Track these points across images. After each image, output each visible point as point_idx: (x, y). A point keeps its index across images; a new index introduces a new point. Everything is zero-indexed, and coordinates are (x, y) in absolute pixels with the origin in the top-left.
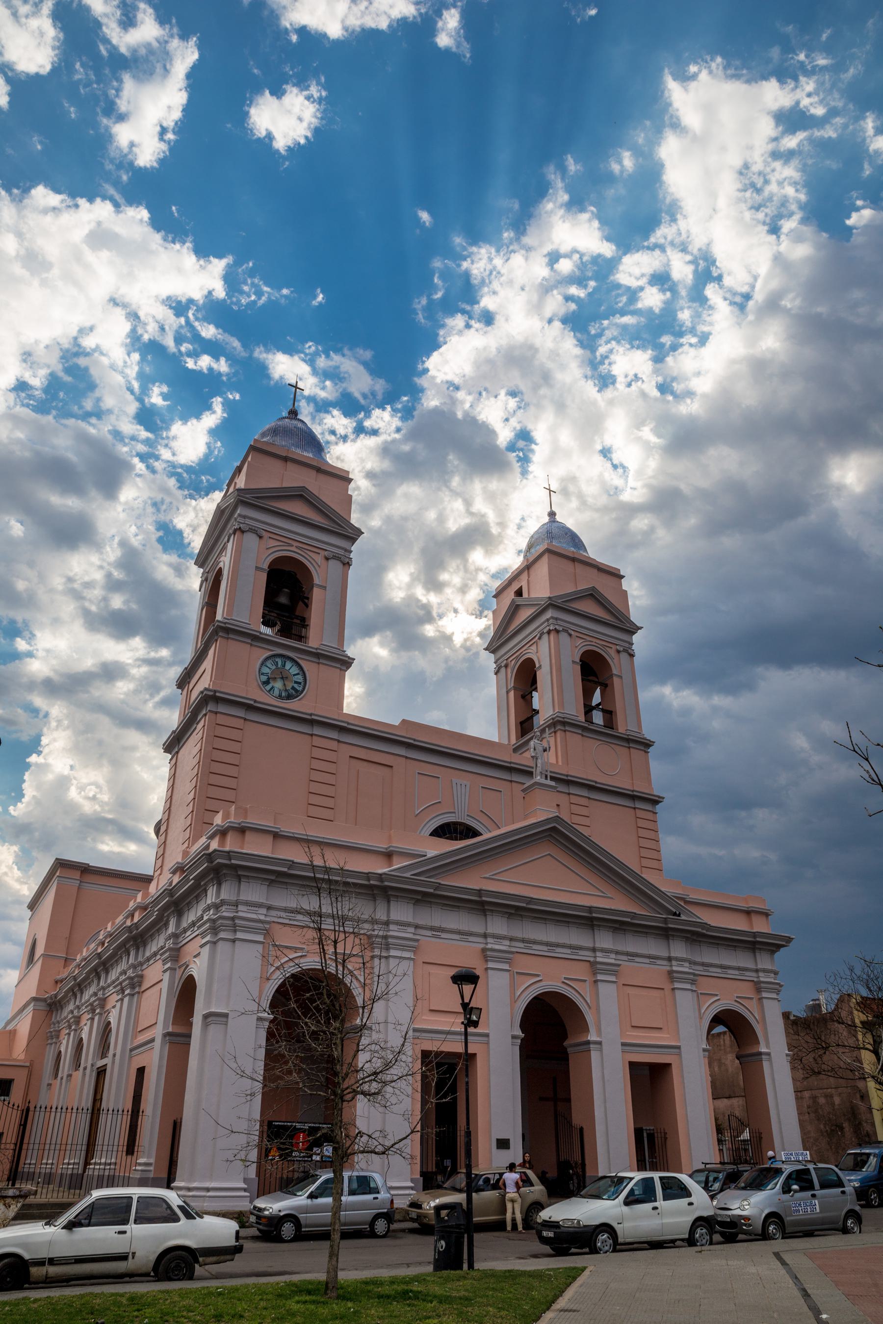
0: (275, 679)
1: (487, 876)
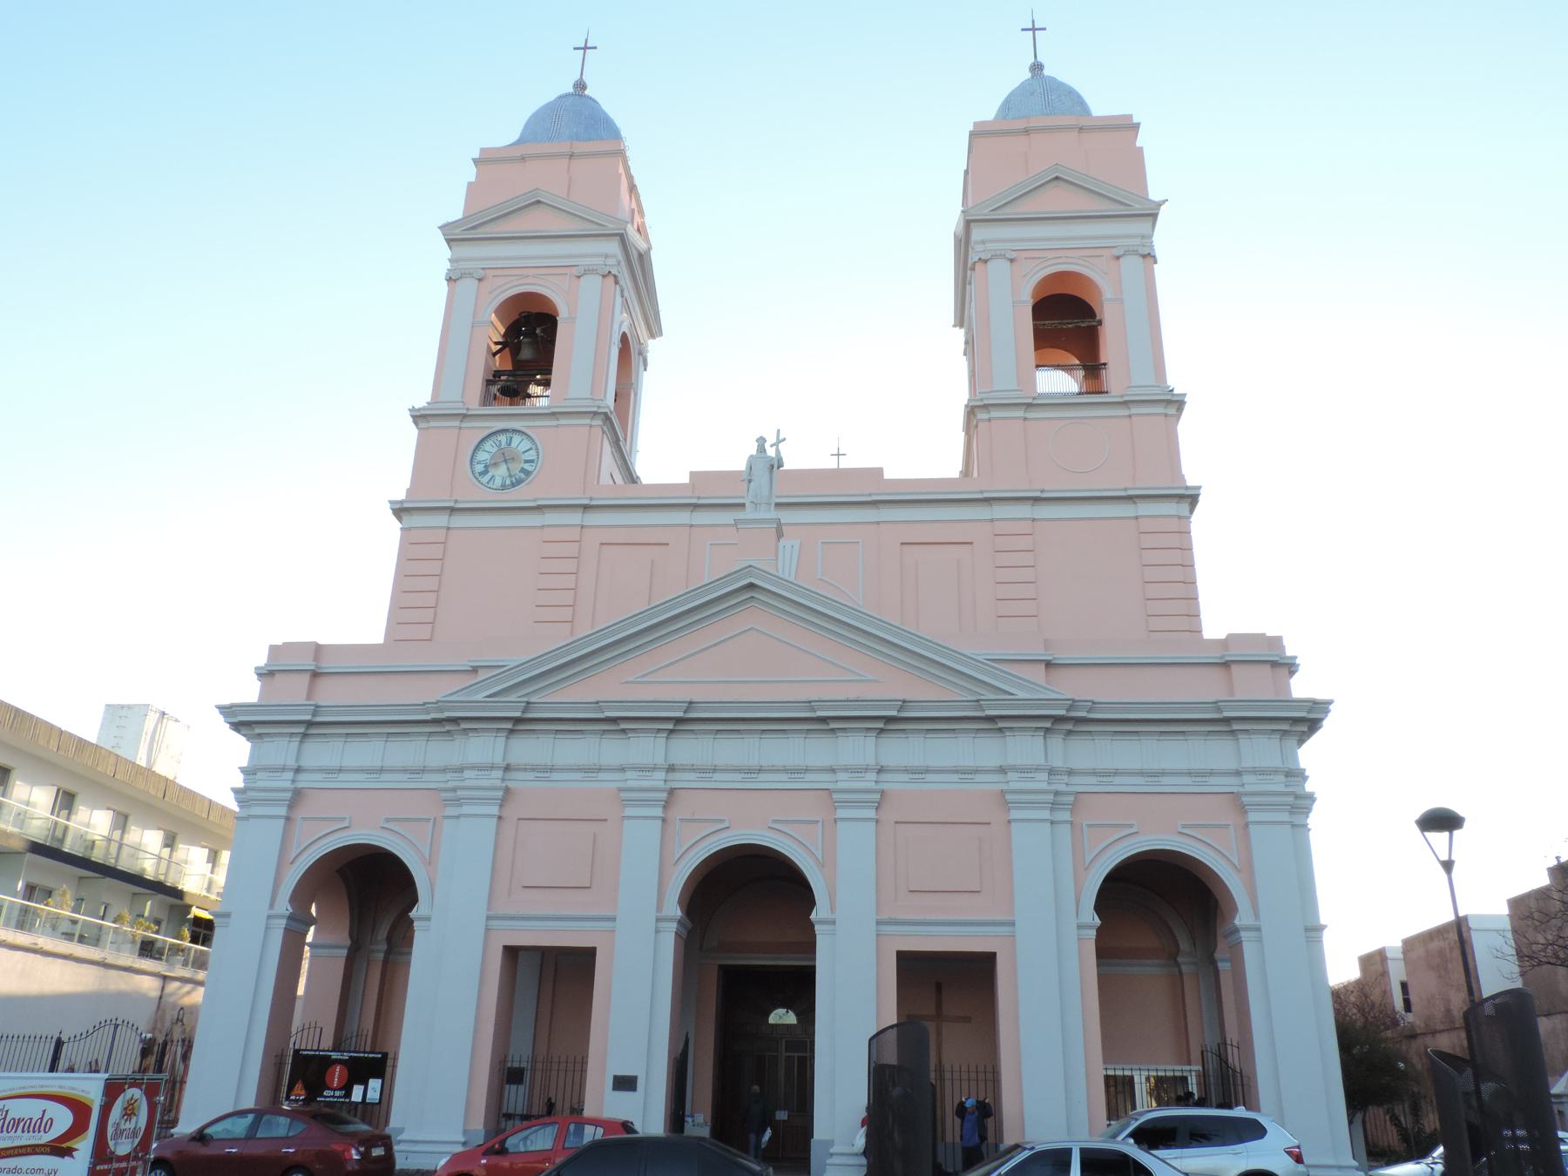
0: (496, 465)
1: (630, 679)
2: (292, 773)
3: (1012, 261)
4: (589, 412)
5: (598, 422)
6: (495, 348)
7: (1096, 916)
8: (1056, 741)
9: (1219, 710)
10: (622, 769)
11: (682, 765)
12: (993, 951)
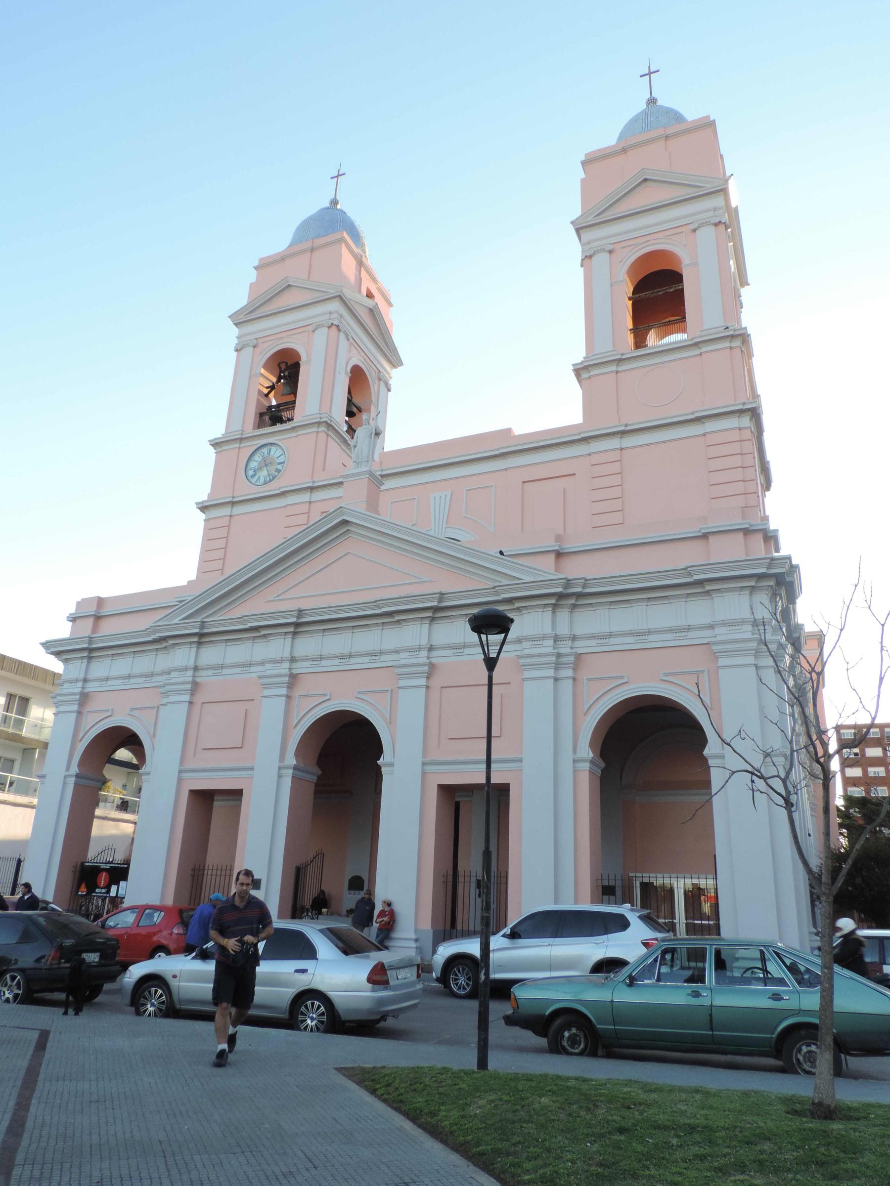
0: (260, 469)
2: (81, 683)
3: (610, 252)
4: (316, 423)
5: (323, 428)
6: (266, 391)
7: (590, 751)
8: (563, 615)
9: (690, 575)
10: (263, 663)
11: (300, 657)
12: (507, 782)
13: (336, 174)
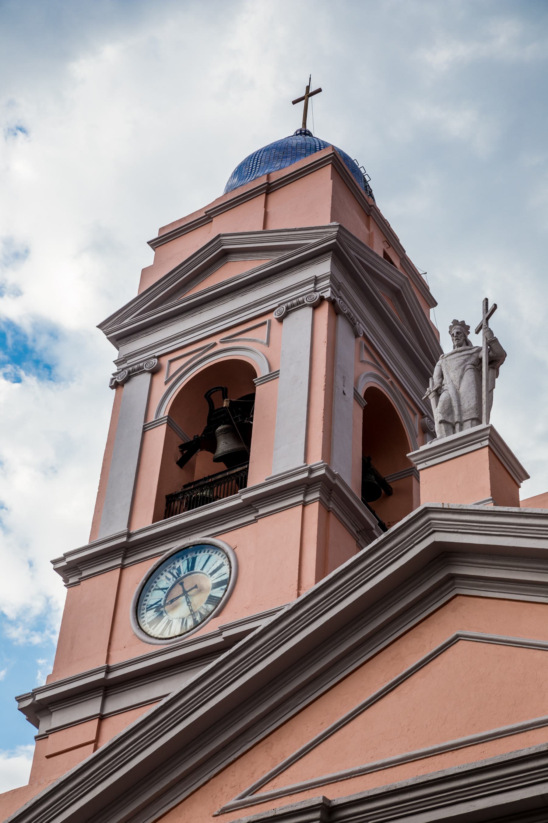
13: (303, 94)
